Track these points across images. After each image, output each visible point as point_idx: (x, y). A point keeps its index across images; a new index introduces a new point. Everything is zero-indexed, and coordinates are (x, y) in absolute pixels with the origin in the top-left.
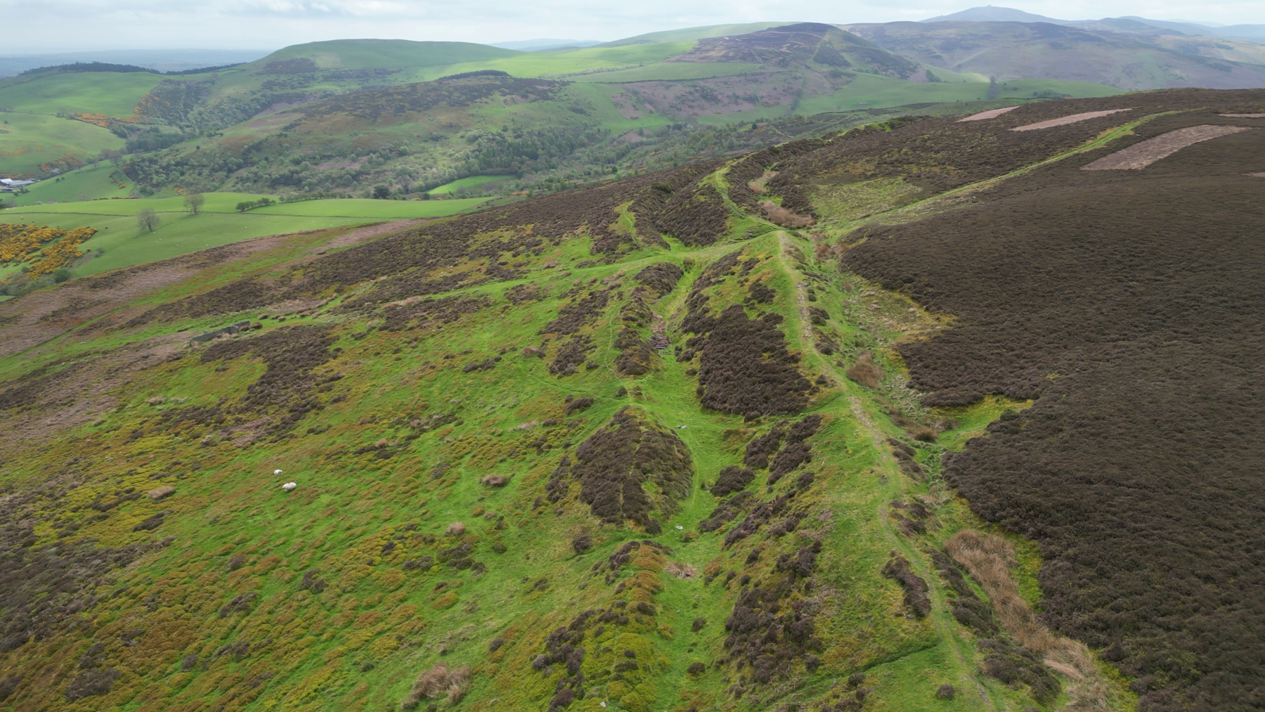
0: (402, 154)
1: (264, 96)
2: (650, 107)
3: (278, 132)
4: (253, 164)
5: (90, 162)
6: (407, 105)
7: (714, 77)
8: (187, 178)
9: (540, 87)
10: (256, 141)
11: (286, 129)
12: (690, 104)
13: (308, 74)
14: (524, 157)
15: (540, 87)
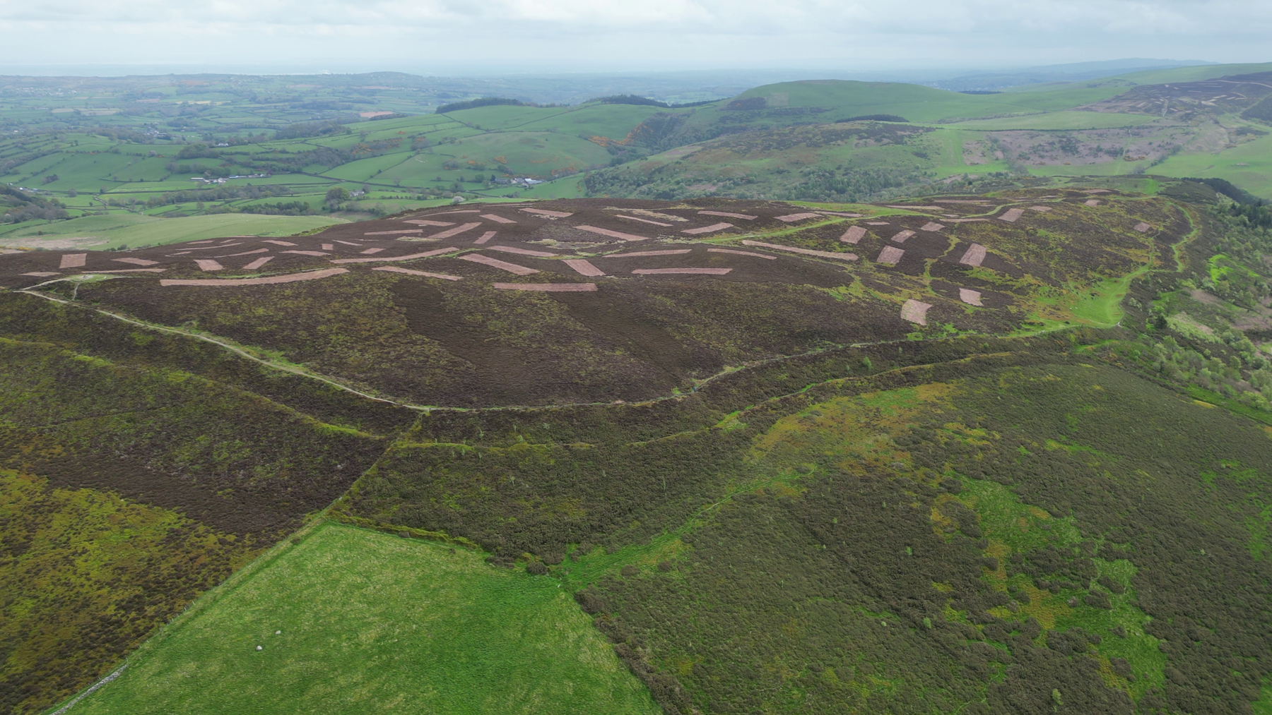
0: (750, 182)
1: (717, 128)
2: (999, 154)
3: (675, 161)
4: (653, 182)
5: (581, 171)
6: (775, 144)
7: (1093, 129)
8: (614, 189)
9: (899, 133)
10: (660, 166)
11: (684, 158)
12: (1042, 153)
13: (756, 111)
14: (833, 191)
15: (899, 133)
